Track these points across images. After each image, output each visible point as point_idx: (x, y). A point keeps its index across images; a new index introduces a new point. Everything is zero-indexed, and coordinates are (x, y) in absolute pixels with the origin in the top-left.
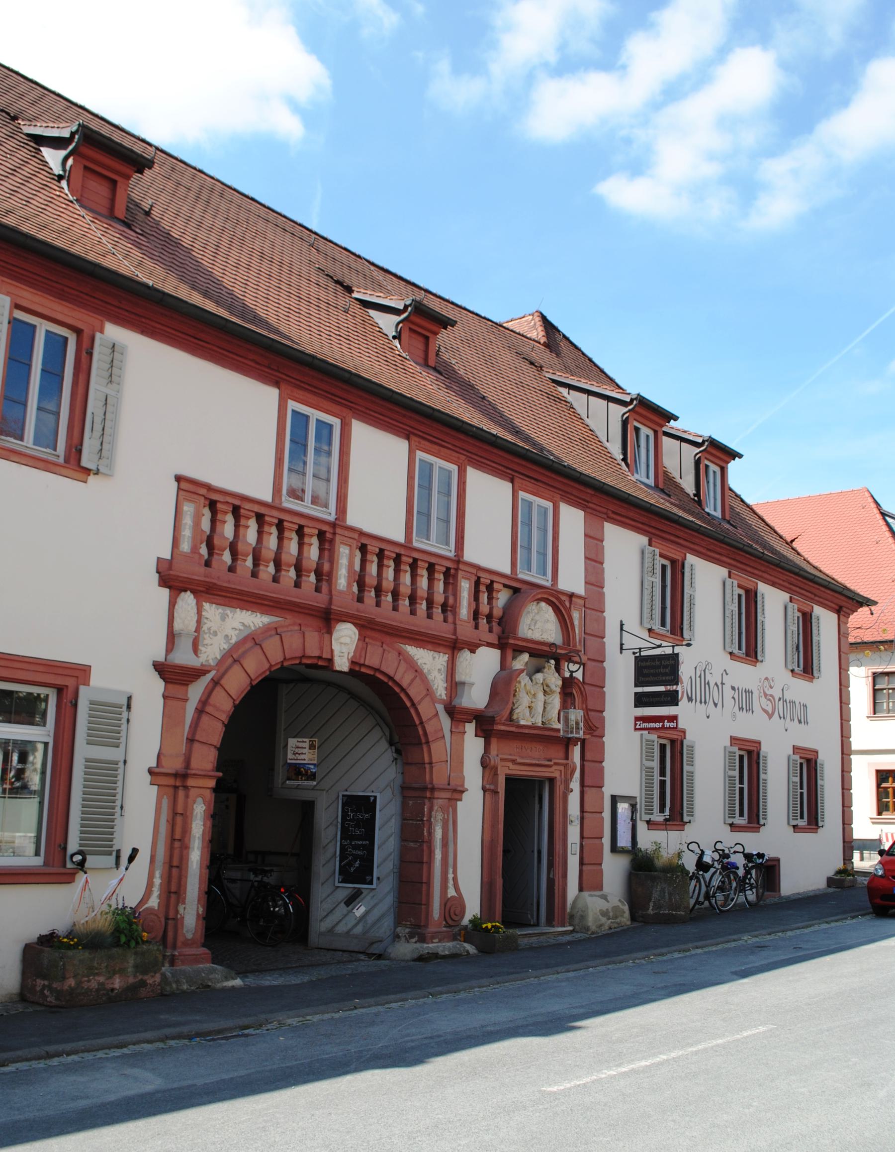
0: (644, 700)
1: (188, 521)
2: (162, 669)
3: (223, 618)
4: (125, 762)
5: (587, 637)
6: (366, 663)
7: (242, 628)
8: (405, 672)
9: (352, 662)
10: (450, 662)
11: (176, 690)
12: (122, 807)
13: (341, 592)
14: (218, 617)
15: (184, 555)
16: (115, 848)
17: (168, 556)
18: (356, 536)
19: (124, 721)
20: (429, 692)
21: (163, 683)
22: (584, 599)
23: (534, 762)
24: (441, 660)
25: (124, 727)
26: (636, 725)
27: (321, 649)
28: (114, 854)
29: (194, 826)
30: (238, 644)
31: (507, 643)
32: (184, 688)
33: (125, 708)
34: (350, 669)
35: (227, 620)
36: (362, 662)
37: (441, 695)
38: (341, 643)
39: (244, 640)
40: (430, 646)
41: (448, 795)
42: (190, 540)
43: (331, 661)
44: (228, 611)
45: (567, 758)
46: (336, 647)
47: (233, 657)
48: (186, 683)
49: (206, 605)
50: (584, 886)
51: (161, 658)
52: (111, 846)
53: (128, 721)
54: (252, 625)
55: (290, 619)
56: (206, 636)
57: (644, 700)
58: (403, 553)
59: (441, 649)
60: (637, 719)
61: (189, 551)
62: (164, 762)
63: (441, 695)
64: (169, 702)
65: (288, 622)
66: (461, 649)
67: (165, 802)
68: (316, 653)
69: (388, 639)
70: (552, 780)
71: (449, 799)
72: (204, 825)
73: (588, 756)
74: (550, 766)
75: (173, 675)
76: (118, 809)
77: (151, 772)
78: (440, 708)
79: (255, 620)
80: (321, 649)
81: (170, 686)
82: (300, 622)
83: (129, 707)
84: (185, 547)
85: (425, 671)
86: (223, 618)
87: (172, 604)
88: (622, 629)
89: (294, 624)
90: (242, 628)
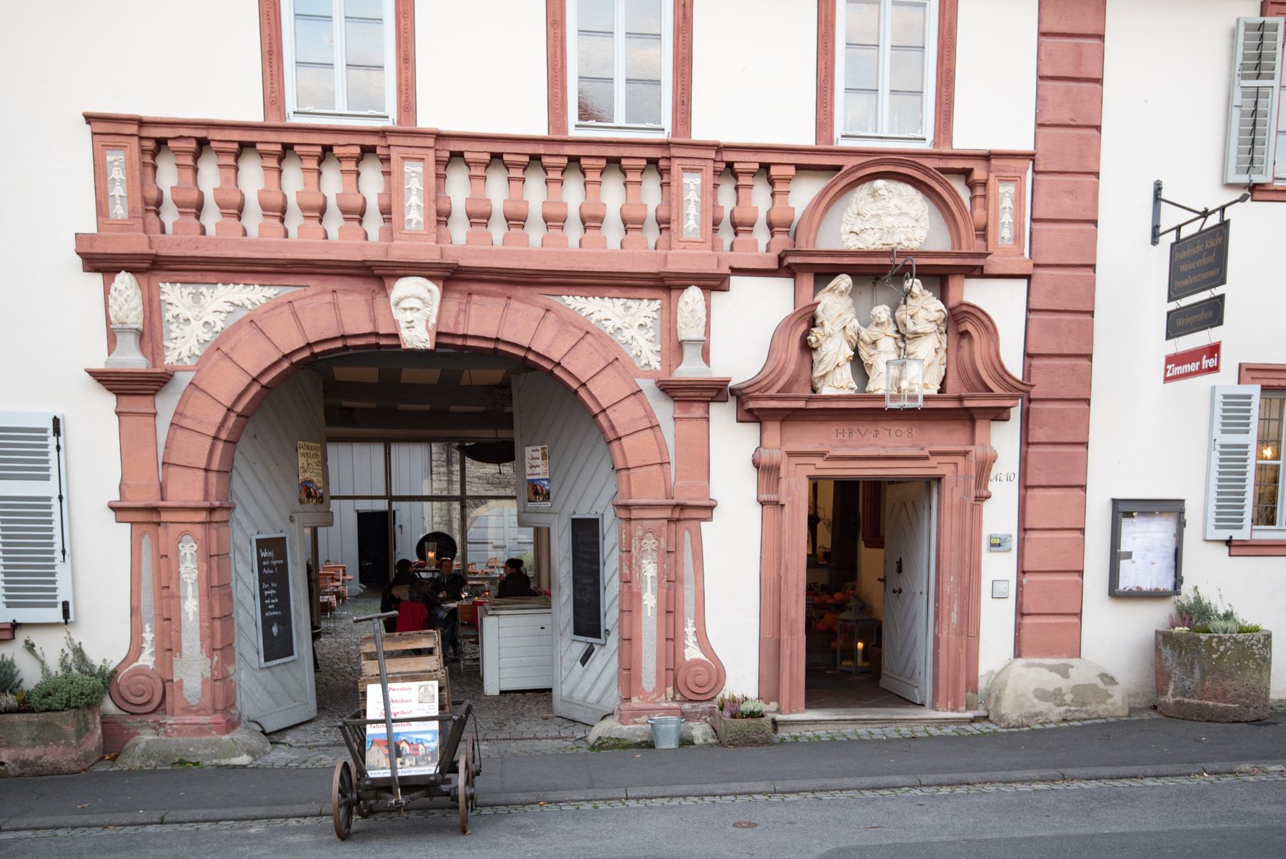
0: (1180, 322)
1: (117, 173)
2: (105, 379)
3: (196, 298)
4: (61, 498)
5: (1037, 226)
6: (471, 332)
7: (231, 309)
8: (555, 338)
9: (439, 334)
10: (666, 311)
11: (141, 404)
12: (64, 552)
13: (413, 235)
14: (188, 300)
15: (121, 226)
16: (60, 600)
17: (90, 227)
18: (431, 142)
19: (52, 449)
20: (616, 361)
21: (114, 397)
22: (1031, 156)
23: (882, 453)
24: (646, 309)
25: (53, 455)
26: (1166, 370)
27: (374, 321)
28: (60, 606)
29: (182, 569)
30: (225, 335)
31: (807, 268)
32: (150, 398)
33: (50, 432)
34: (438, 345)
35: (203, 301)
36: (461, 332)
37: (648, 364)
38: (405, 309)
39: (238, 326)
40: (614, 292)
41: (667, 513)
42: (125, 200)
43: (396, 336)
44: (203, 289)
45: (973, 443)
46: (401, 317)
47: (218, 348)
48: (154, 393)
49: (166, 287)
50: (1024, 647)
51: (100, 364)
52: (55, 597)
53: (58, 448)
54: (247, 303)
55: (314, 284)
56: (173, 327)
57: (1180, 322)
58: (541, 152)
59: (641, 293)
60: (1173, 360)
61: (126, 216)
62: (128, 496)
63: (648, 364)
64: (126, 419)
65: (310, 291)
66: (683, 288)
67: (146, 542)
68: (368, 329)
69: (521, 292)
70: (939, 479)
71: (670, 520)
72: (198, 569)
73: (1037, 434)
74: (926, 458)
75: (131, 387)
76: (58, 555)
77: (114, 509)
78: (647, 385)
79: (253, 295)
80: (374, 321)
81: (124, 399)
82: (334, 287)
83: (57, 431)
84: (119, 211)
85: (610, 330)
86: (196, 298)
87: (107, 292)
88: (1157, 199)
89: (323, 292)
90: (231, 309)
